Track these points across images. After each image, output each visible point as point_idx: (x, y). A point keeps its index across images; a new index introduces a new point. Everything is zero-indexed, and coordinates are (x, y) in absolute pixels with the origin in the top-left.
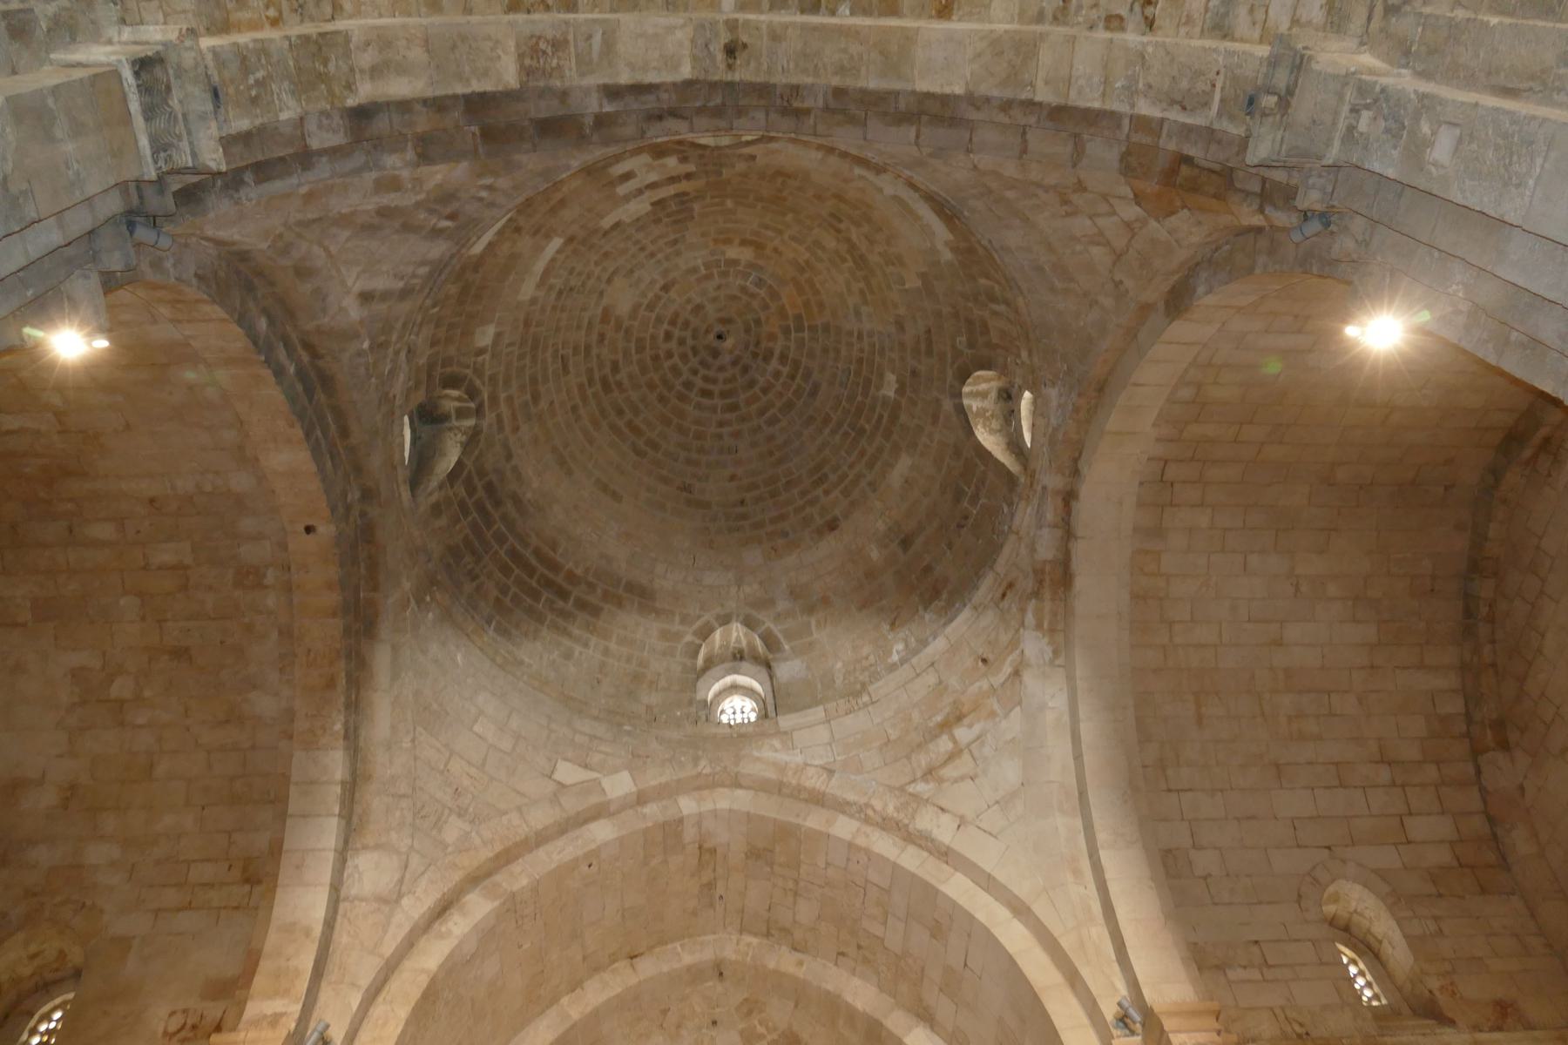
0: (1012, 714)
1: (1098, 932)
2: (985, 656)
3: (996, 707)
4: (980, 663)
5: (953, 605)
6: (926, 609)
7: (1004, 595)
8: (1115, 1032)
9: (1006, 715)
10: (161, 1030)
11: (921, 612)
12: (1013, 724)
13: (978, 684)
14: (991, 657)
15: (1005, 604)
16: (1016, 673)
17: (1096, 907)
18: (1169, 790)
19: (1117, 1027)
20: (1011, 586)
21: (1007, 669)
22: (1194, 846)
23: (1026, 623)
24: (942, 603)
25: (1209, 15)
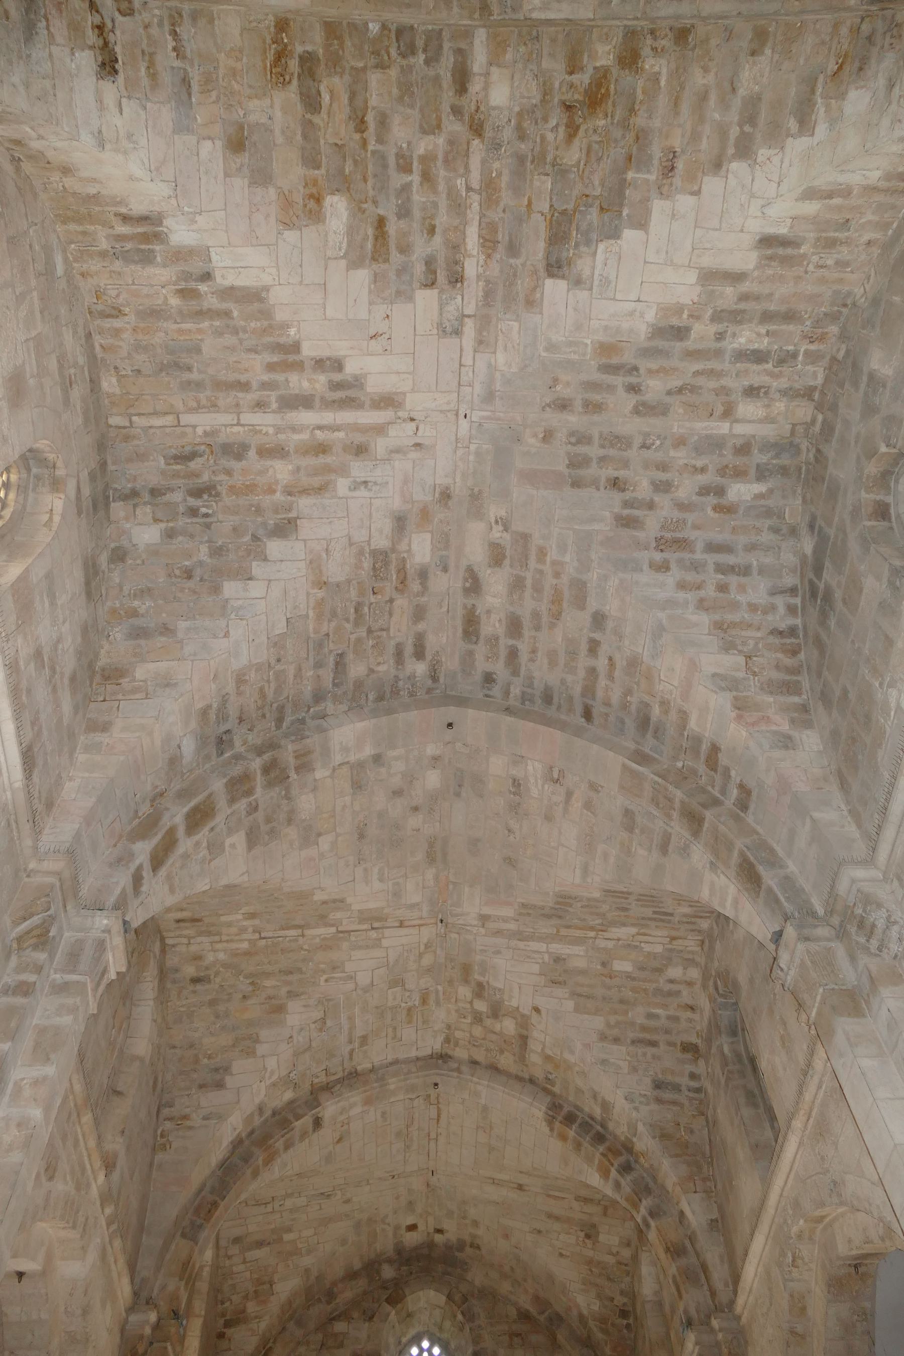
25: (43, 12)
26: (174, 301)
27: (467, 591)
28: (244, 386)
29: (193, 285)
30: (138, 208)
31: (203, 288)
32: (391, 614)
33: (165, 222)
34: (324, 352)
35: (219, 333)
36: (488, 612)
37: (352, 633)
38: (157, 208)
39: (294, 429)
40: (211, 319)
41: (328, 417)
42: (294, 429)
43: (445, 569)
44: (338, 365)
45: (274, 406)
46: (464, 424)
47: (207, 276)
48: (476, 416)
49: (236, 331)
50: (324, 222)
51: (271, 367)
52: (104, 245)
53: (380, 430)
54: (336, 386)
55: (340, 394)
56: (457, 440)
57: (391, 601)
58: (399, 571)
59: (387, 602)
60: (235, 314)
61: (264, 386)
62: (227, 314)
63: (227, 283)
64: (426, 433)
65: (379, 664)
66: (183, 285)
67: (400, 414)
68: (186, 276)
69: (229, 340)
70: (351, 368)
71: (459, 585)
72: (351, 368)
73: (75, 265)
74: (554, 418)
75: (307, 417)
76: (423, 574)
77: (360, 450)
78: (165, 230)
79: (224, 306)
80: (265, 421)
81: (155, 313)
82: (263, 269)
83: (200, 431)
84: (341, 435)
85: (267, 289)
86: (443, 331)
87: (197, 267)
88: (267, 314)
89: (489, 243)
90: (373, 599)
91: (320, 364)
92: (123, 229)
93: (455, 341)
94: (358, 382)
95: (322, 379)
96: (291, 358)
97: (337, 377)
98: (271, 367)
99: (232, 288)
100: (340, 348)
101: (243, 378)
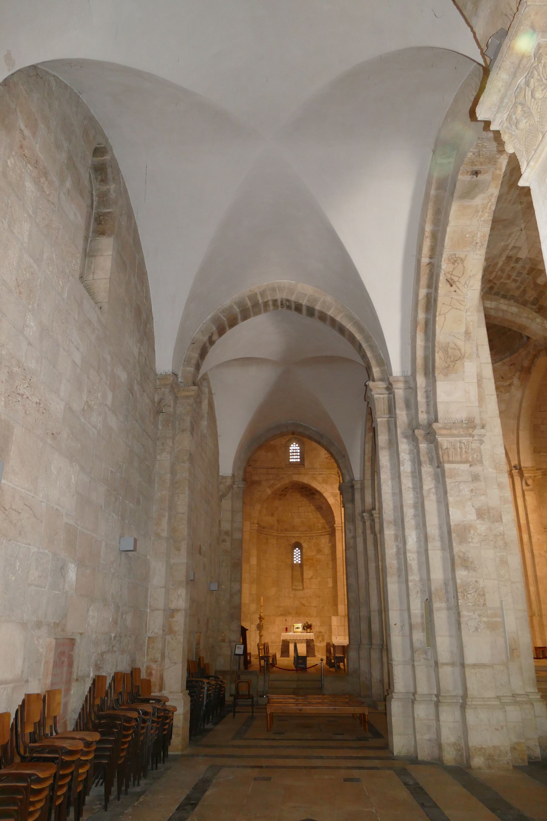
0: (507, 394)
1: (515, 447)
2: (503, 376)
3: (503, 390)
4: (501, 378)
8: (513, 469)
9: (505, 393)
10: (324, 456)
13: (500, 383)
15: (512, 367)
16: (510, 385)
17: (515, 441)
19: (514, 467)
20: (514, 364)
21: (508, 383)
93: (516, 245)
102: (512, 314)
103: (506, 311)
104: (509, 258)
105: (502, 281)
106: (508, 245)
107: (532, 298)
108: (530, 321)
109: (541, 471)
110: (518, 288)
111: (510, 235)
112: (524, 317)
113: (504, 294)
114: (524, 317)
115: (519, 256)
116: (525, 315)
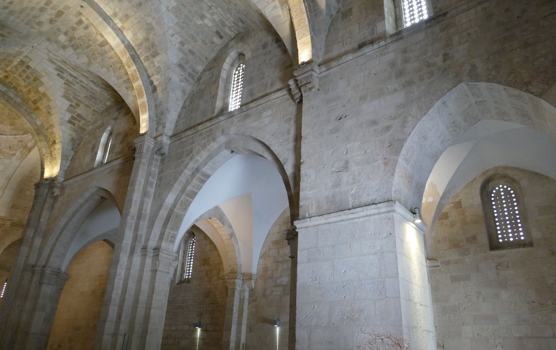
4: (9, 147)
5: (14, 130)
6: (9, 125)
7: (20, 141)
9: (7, 159)
11: (8, 125)
12: (7, 161)
13: (6, 150)
14: (11, 148)
16: (13, 155)
18: (30, 181)
20: (22, 141)
21: (12, 153)
22: (28, 190)
23: (20, 150)
24: (12, 128)
26: (82, 106)
27: (56, 21)
28: (82, 86)
29: (75, 106)
30: (70, 125)
31: (74, 104)
32: (81, 37)
33: (68, 120)
34: (60, 79)
35: (79, 96)
36: (51, 14)
37: (93, 46)
38: (66, 123)
39: (78, 75)
40: (77, 99)
41: (68, 70)
42: (78, 75)
43: (59, 29)
44: (58, 75)
45: (79, 79)
46: (35, 45)
47: (71, 105)
48: (30, 44)
49: (75, 94)
50: (44, 92)
51: (73, 84)
52: (83, 121)
53: (58, 60)
54: (62, 72)
55: (63, 71)
56: (38, 45)
57: (79, 39)
58: (72, 41)
59: (80, 40)
60: (72, 96)
61: (78, 83)
62: (74, 97)
63: (68, 102)
64: (47, 52)
65: (93, 32)
66: (77, 107)
67: (50, 58)
68: (75, 108)
69: (78, 94)
70: (57, 72)
71: (58, 23)
72: (57, 72)
73: (92, 121)
74: (6, 34)
75: (73, 74)
76: (66, 34)
77: (65, 62)
78: (70, 118)
79: (73, 99)
80: (83, 79)
81: (87, 106)
82: (59, 100)
83: (98, 88)
84: (67, 66)
85: (62, 96)
86: (31, 60)
87: (71, 108)
88: (66, 92)
89: (11, 62)
90: (83, 44)
91: (62, 78)
92: (77, 122)
93: (28, 55)
94: (56, 69)
95: (65, 75)
96: (68, 83)
97: (61, 73)
98: (73, 84)
99: (68, 101)
100: (56, 77)
101: (81, 87)
102: (15, 102)
103: (12, 98)
104: (22, 62)
105: (15, 75)
106: (22, 52)
107: (33, 99)
108: (26, 113)
109: (11, 222)
110: (26, 87)
111: (24, 46)
112: (24, 109)
113: (15, 86)
114: (24, 109)
115: (29, 64)
116: (24, 108)
